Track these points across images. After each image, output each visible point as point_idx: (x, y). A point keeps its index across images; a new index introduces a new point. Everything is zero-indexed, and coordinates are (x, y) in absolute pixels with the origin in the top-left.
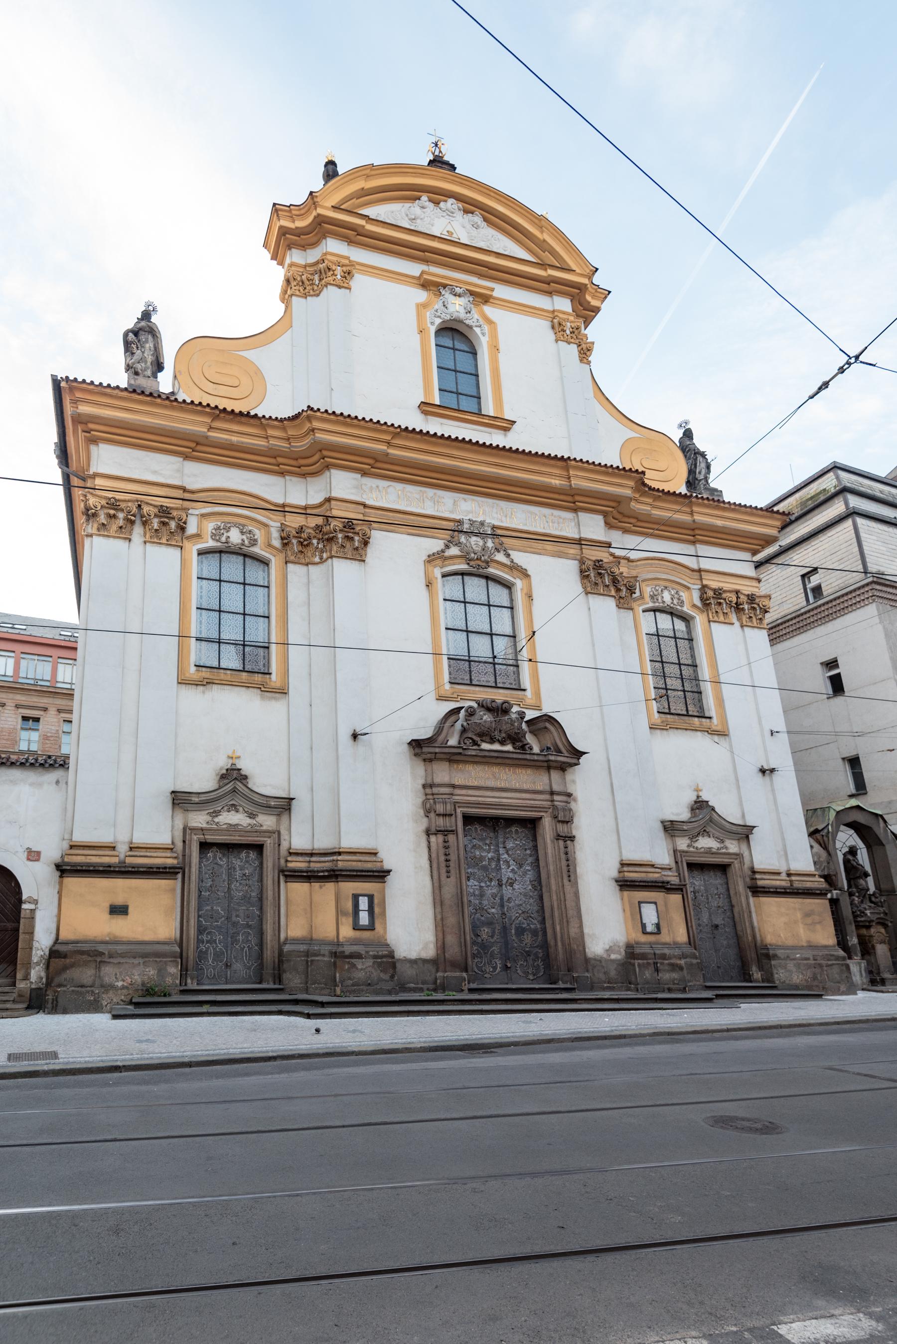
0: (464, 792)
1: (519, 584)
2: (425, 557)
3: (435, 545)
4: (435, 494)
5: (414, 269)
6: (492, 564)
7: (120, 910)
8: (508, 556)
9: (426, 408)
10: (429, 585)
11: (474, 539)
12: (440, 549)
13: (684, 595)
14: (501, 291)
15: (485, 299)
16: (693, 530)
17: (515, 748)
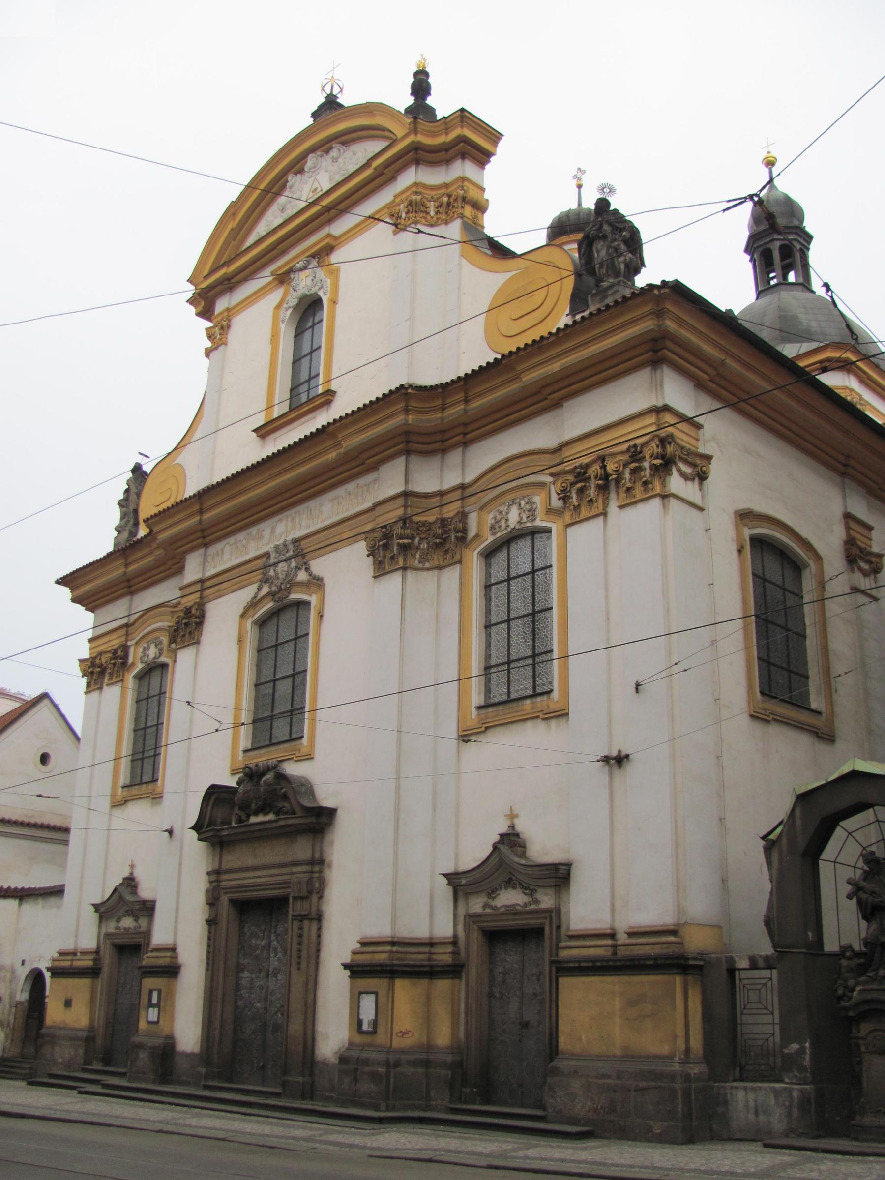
0: (233, 876)
1: (314, 600)
2: (241, 611)
3: (247, 594)
4: (258, 530)
5: (265, 277)
6: (294, 588)
7: (68, 1003)
8: (307, 570)
9: (264, 432)
10: (240, 641)
11: (280, 565)
12: (252, 595)
13: (538, 500)
14: (338, 228)
15: (329, 249)
16: (538, 393)
17: (277, 813)
